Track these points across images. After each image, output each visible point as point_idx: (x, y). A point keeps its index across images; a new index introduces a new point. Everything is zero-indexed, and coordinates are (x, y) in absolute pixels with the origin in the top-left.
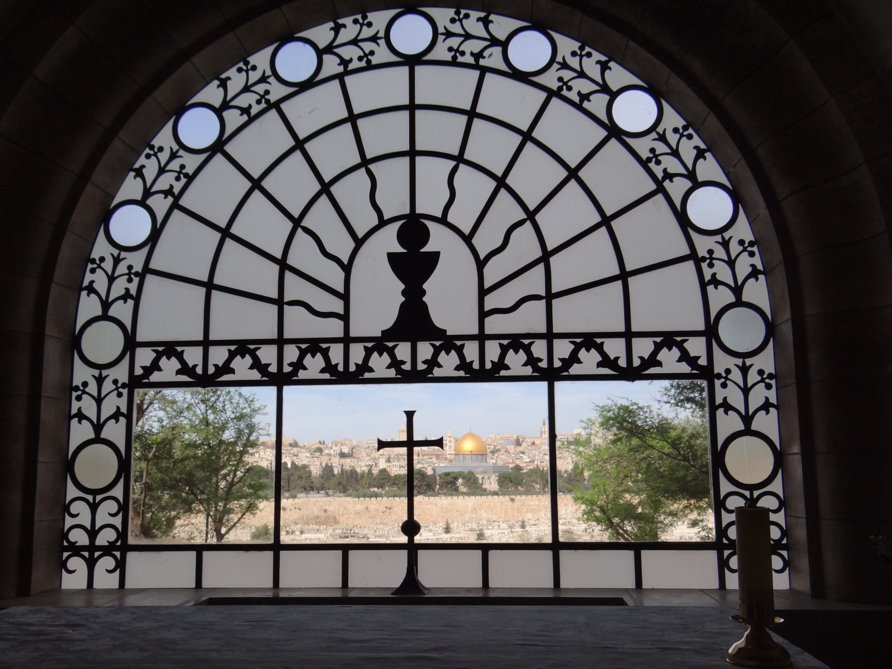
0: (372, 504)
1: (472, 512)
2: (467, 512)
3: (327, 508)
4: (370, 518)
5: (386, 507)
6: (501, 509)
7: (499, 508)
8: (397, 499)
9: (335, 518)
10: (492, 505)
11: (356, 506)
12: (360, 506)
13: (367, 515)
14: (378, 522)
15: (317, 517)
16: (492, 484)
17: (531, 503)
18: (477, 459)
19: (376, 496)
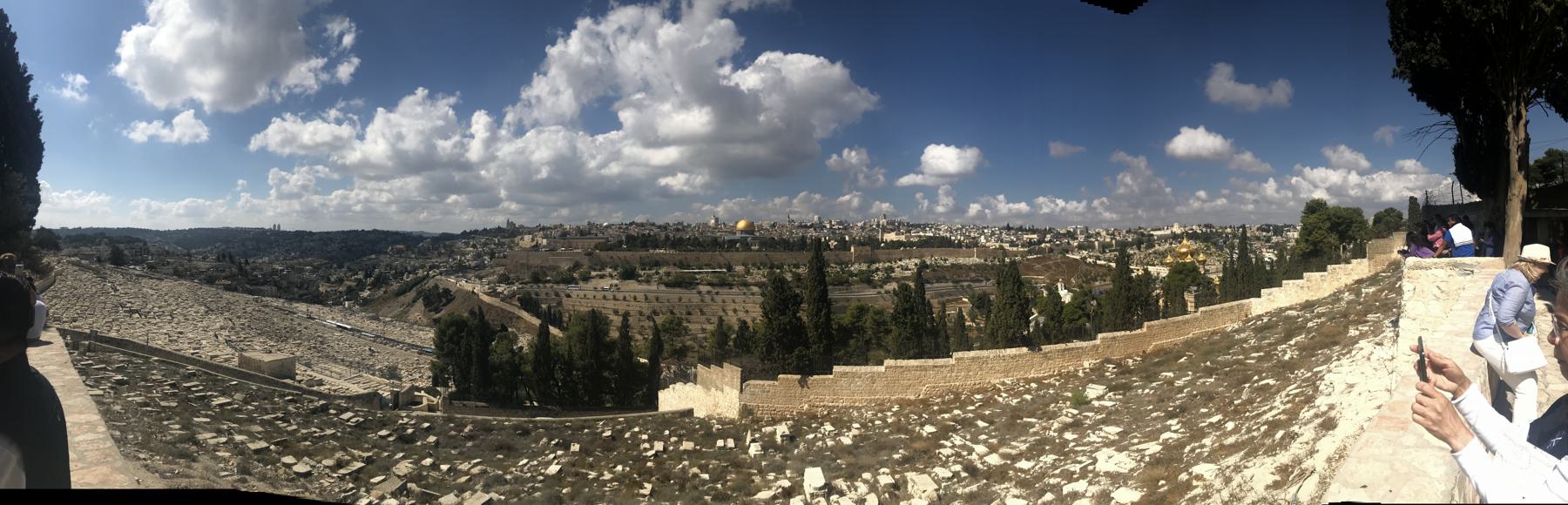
8: (702, 253)
19: (691, 251)
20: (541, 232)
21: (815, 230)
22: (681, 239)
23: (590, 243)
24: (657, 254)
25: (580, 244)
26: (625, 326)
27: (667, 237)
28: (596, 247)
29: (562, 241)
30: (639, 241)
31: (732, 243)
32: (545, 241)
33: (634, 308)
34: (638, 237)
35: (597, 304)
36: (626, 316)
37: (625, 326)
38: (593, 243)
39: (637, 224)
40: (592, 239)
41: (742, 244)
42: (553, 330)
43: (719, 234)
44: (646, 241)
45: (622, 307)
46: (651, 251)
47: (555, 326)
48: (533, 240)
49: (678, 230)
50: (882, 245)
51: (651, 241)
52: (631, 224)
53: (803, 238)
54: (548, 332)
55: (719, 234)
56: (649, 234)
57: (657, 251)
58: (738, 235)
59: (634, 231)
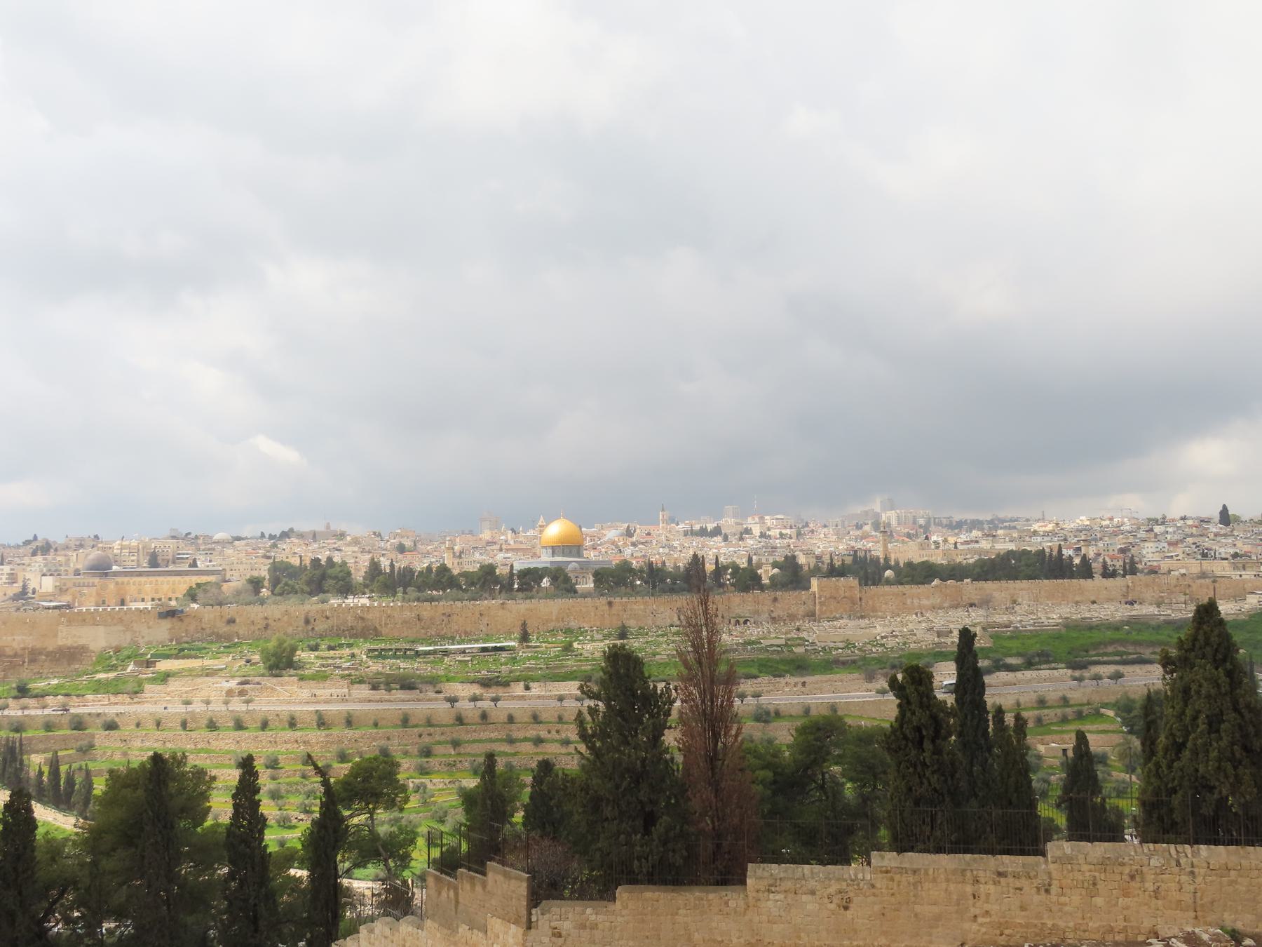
0: (426, 610)
1: (557, 620)
2: (552, 621)
3: (365, 616)
4: (423, 628)
5: (444, 614)
6: (595, 615)
7: (593, 614)
8: (459, 604)
9: (375, 629)
10: (584, 610)
11: (405, 613)
12: (409, 614)
13: (418, 625)
14: (433, 633)
15: (352, 628)
16: (588, 585)
17: (635, 607)
18: (570, 552)
19: (432, 599)
20: (39, 558)
21: (726, 539)
22: (408, 572)
23: (173, 588)
24: (349, 609)
25: (148, 587)
26: (246, 792)
27: (375, 567)
28: (192, 596)
29: (96, 580)
30: (304, 578)
31: (529, 579)
32: (48, 584)
33: (286, 746)
34: (302, 568)
35: (168, 743)
36: (247, 764)
37: (246, 792)
38: (183, 584)
39: (301, 536)
40: (186, 573)
41: (554, 579)
42: (44, 814)
43: (500, 556)
44: (324, 577)
45: (248, 743)
46: (334, 601)
47: (44, 804)
48: (12, 579)
49: (401, 549)
50: (888, 573)
51: (335, 578)
52: (285, 535)
53: (697, 562)
54: (31, 824)
55: (500, 556)
56: (330, 559)
57: (350, 601)
58: (545, 559)
59: (295, 554)
